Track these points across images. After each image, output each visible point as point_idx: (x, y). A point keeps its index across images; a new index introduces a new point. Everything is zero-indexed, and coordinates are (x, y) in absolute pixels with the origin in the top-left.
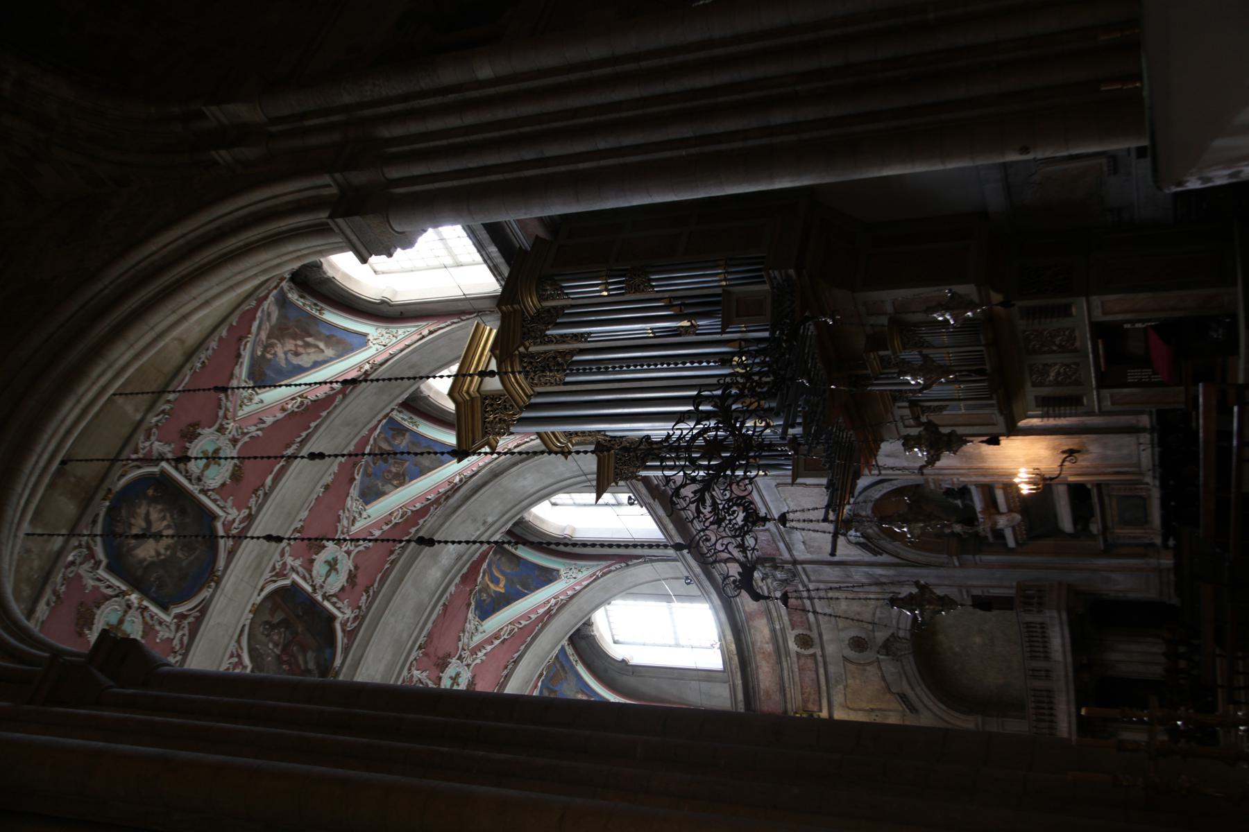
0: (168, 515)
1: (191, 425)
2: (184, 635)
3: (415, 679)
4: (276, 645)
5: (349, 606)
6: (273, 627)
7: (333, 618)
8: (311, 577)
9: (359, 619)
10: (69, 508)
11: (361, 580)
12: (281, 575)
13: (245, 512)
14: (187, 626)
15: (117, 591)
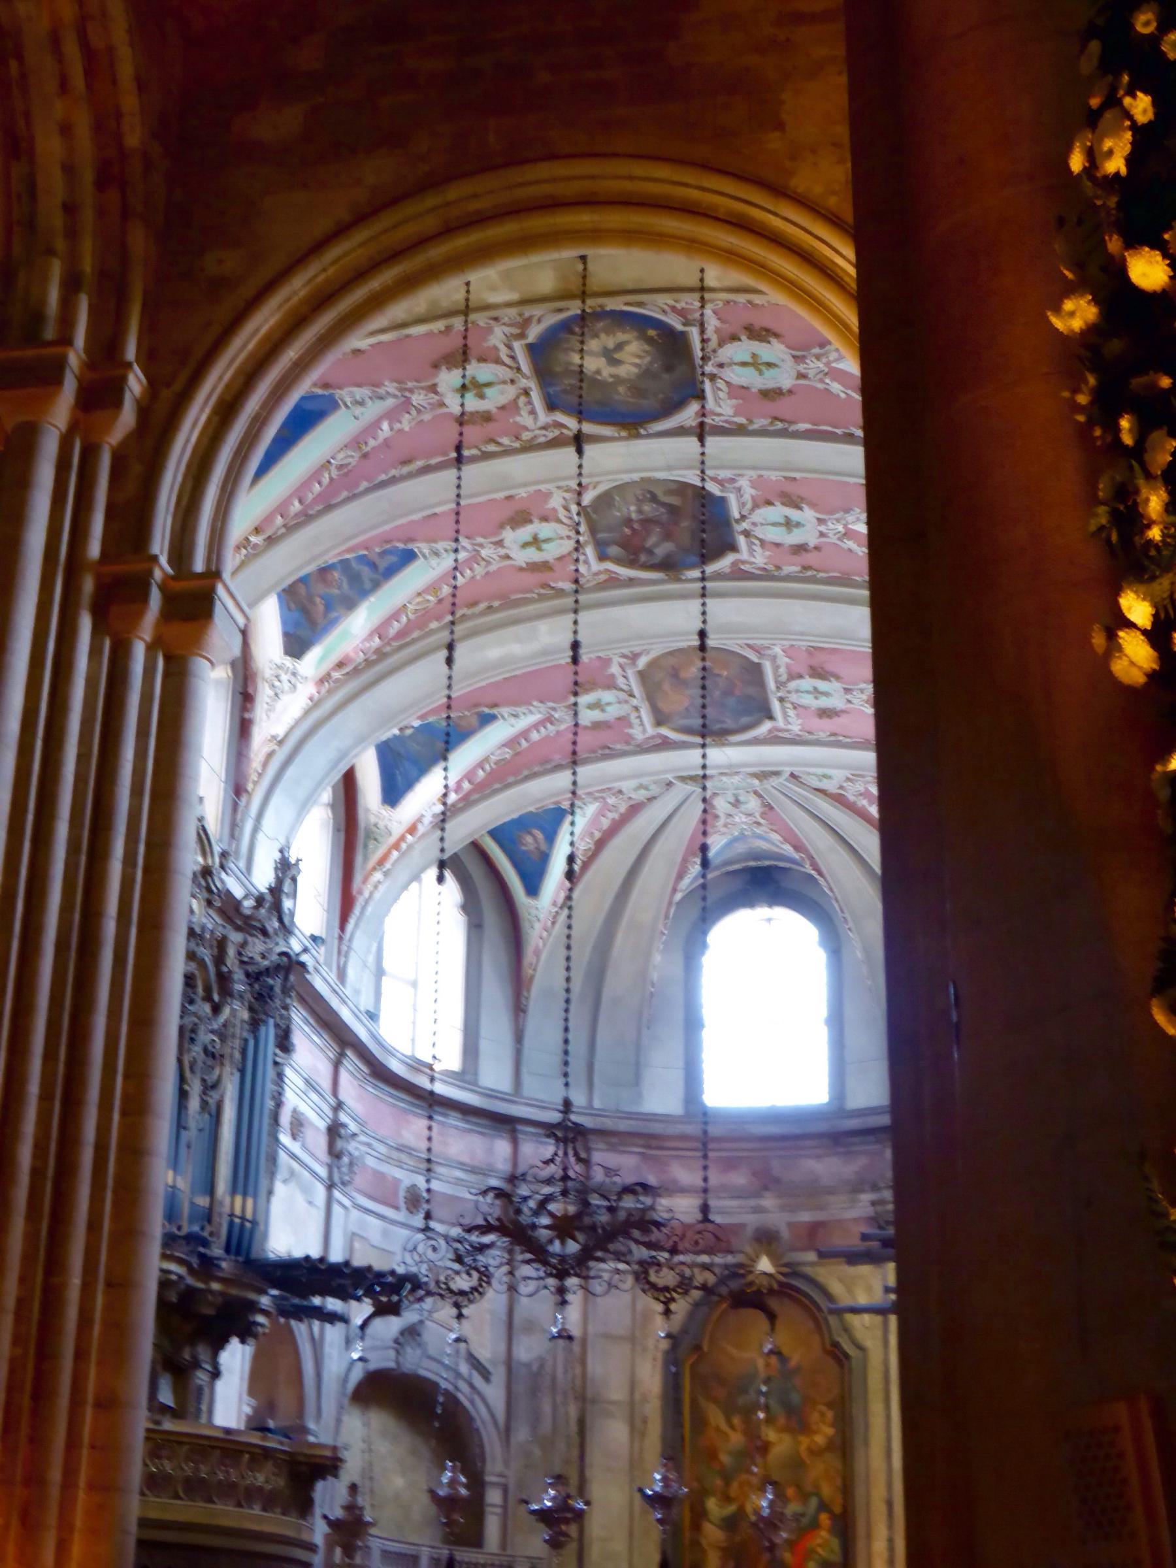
0: (648, 359)
1: (767, 330)
2: (544, 435)
3: (769, 652)
4: (640, 511)
5: (769, 557)
6: (654, 498)
7: (733, 548)
8: (753, 510)
9: (766, 575)
10: (546, 282)
11: (810, 558)
12: (720, 483)
13: (741, 420)
14: (557, 432)
15: (514, 365)
